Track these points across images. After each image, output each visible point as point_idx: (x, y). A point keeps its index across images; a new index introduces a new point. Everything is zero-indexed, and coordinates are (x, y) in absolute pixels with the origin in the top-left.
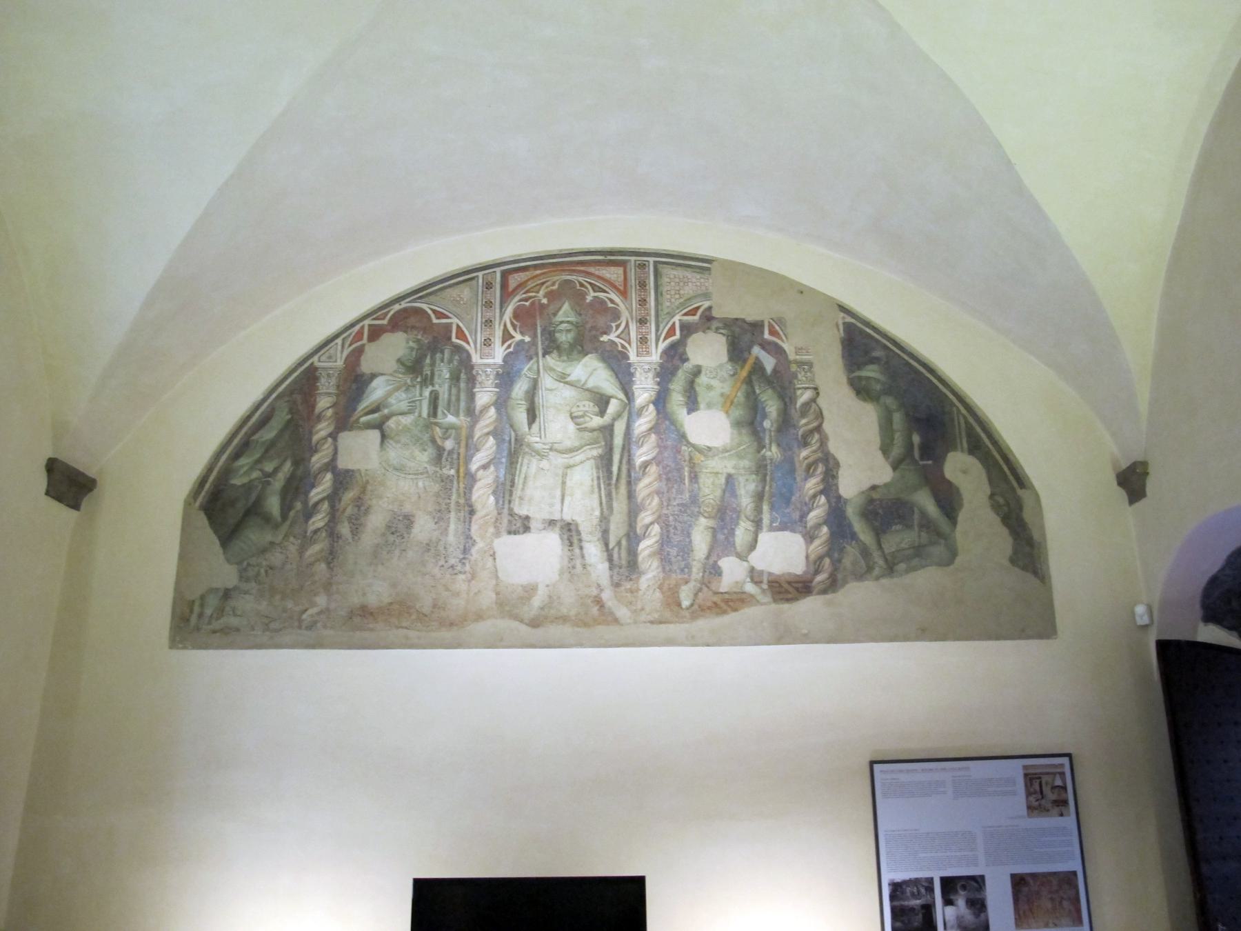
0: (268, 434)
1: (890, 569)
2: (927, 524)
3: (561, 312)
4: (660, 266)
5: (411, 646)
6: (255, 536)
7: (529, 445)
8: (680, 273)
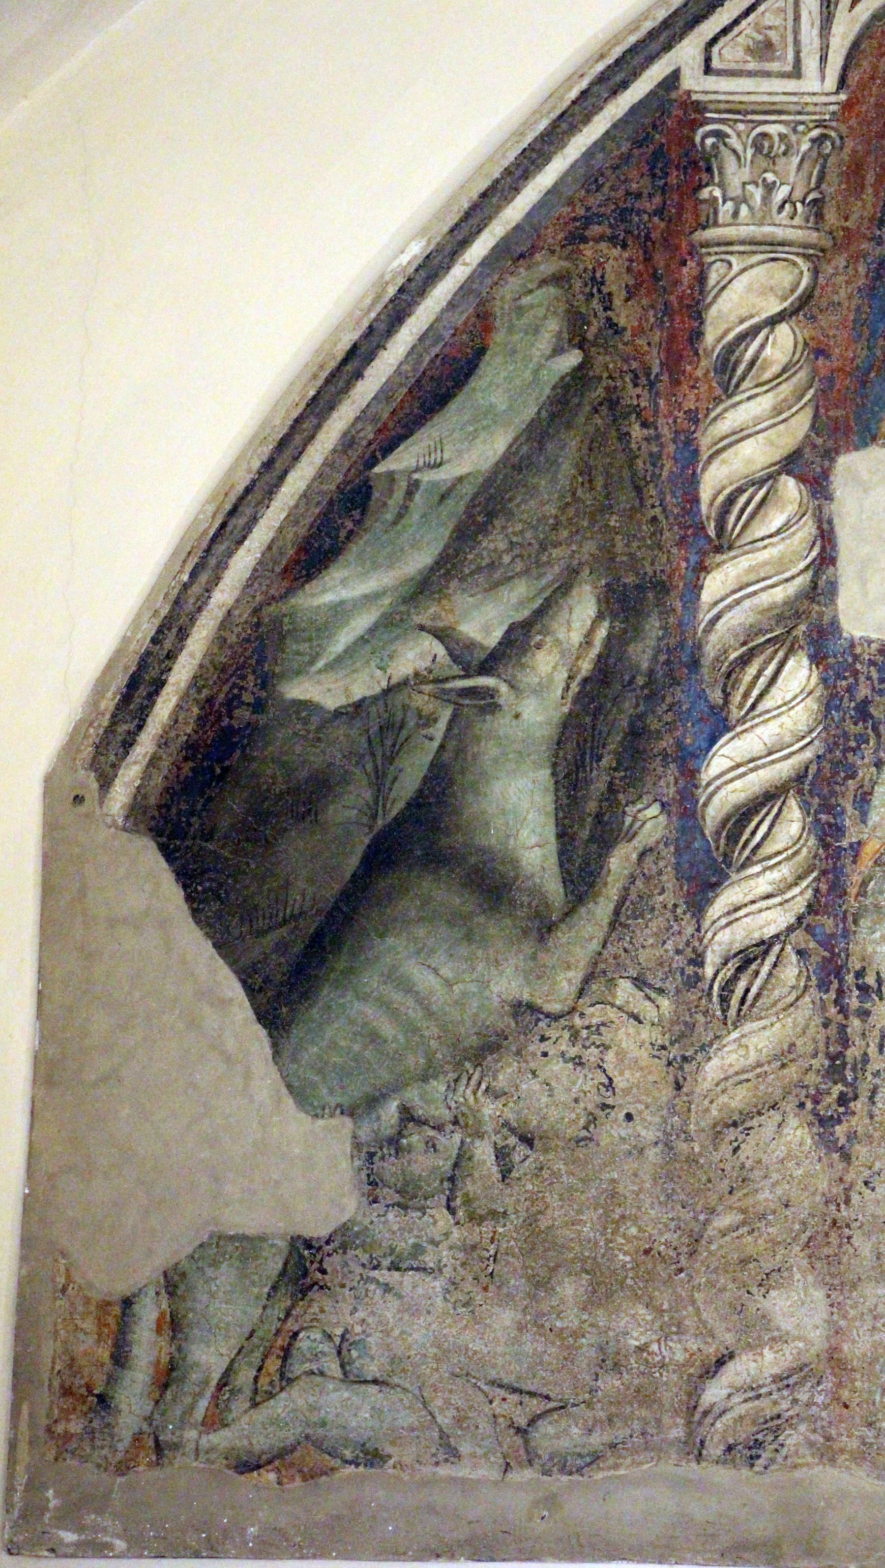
0: (465, 447)
6: (428, 973)
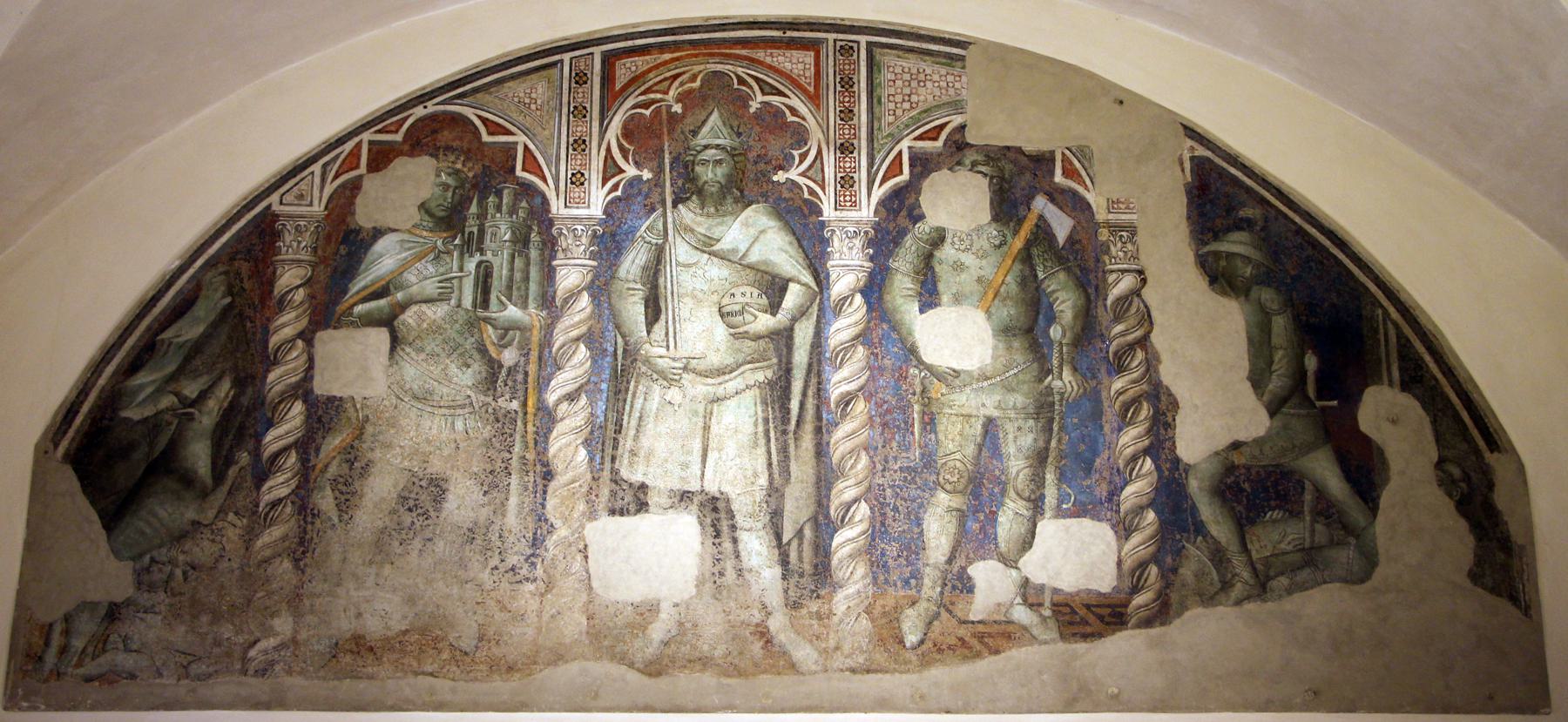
0: (189, 330)
1: (1261, 588)
2: (1326, 509)
3: (705, 129)
4: (877, 51)
5: (440, 707)
6: (165, 511)
7: (647, 361)
8: (911, 63)
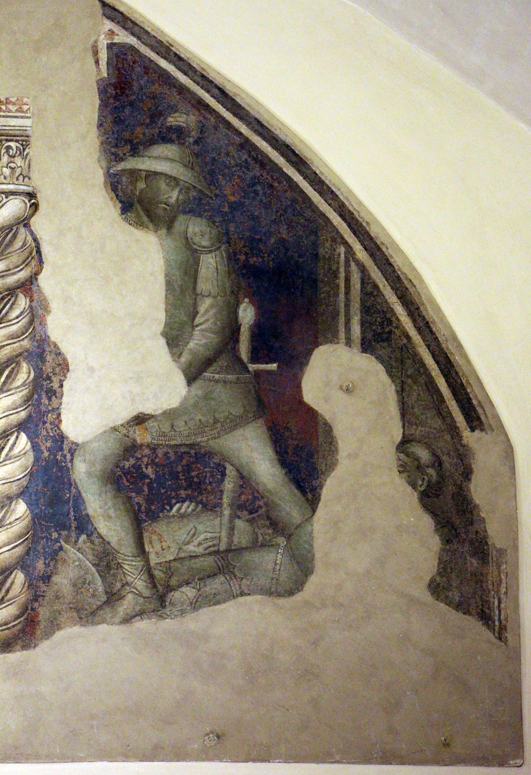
1: (159, 599)
2: (252, 503)
